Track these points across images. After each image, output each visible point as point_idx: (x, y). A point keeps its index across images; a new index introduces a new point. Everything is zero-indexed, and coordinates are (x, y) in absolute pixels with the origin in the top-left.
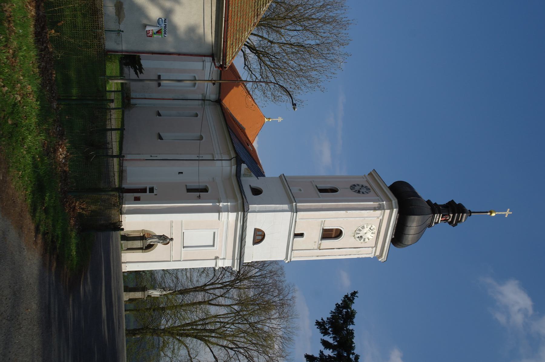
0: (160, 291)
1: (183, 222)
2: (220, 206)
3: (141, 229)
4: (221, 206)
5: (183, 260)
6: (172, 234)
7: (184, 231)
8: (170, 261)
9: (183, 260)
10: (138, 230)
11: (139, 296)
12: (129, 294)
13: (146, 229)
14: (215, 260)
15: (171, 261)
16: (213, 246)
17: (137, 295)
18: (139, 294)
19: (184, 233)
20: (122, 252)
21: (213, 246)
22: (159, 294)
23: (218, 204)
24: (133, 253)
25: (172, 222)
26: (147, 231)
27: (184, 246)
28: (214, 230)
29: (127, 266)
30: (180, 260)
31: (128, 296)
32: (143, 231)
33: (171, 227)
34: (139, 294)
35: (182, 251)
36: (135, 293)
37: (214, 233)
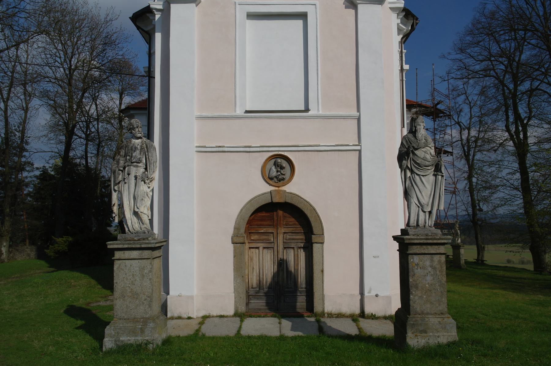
0: (412, 172)
1: (204, 114)
2: (160, 7)
3: (231, 247)
4: (162, 3)
5: (358, 110)
6: (252, 149)
7: (240, 112)
8: (360, 151)
9: (358, 110)
10: (234, 257)
11: (434, 268)
12: (423, 313)
13: (231, 231)
14: (360, 7)
15: (358, 148)
16: (303, 16)
17: (429, 278)
18: (423, 268)
19: (247, 112)
20: (317, 308)
21: (303, 16)
22: (432, 178)
23: (157, 16)
24: (322, 271)
25: (203, 150)
26: (236, 228)
27: (303, 109)
28: (241, 15)
29: (373, 293)
30: (356, 121)
31: (433, 321)
32: (236, 240)
33: (220, 150)
34: (423, 268)
35: (321, 112)
36: (416, 287)
37: (252, 16)
